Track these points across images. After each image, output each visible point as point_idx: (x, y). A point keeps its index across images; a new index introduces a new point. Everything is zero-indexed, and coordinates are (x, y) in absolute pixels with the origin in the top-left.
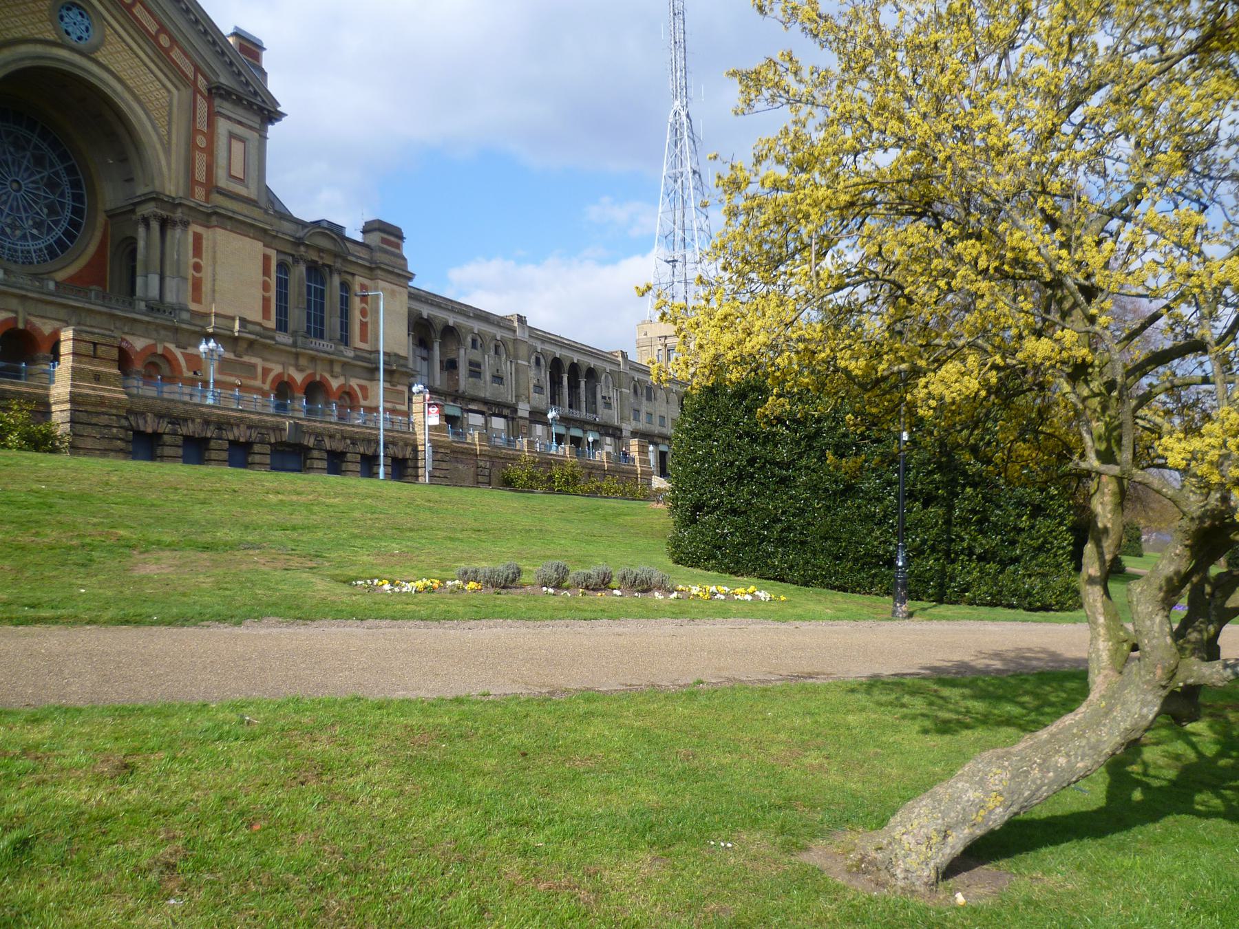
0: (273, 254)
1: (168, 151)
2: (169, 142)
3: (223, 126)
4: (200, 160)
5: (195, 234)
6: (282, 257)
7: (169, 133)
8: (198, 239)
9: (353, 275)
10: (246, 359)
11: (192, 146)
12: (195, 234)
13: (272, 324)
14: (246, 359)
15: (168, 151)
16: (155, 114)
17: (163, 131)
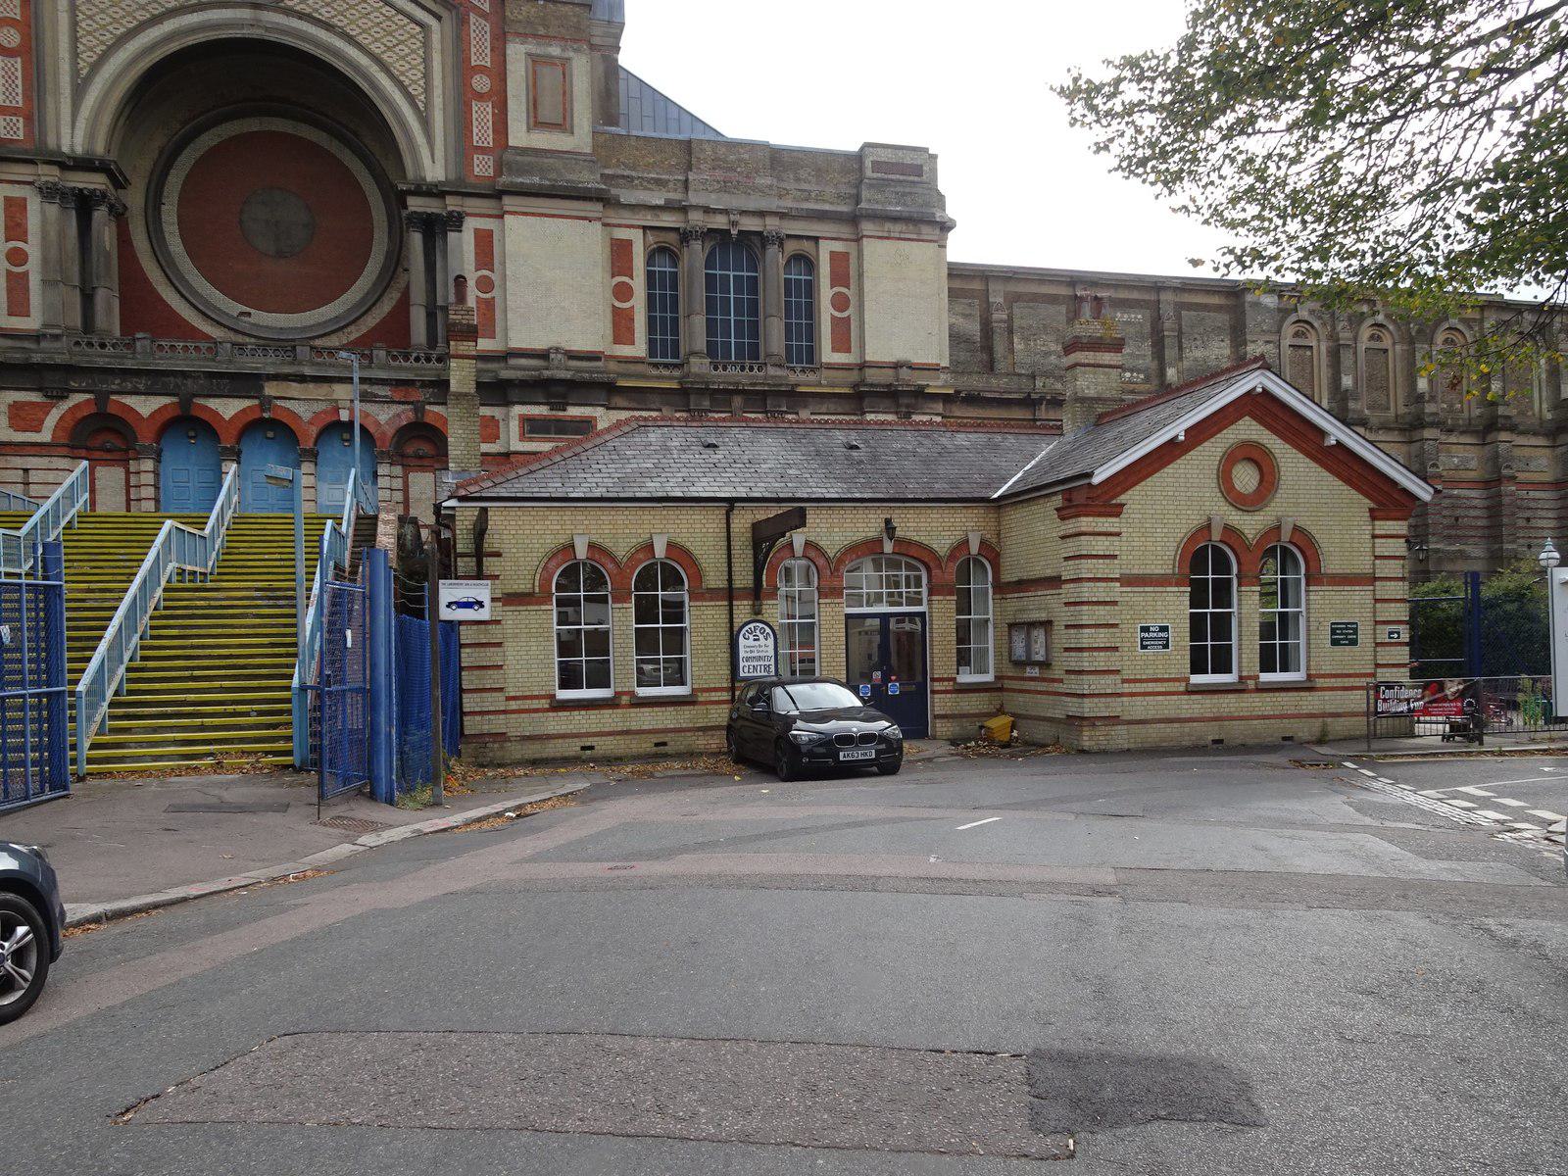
0: (637, 238)
1: (426, 122)
2: (428, 104)
3: (517, 53)
4: (482, 115)
5: (477, 231)
6: (651, 238)
7: (428, 89)
8: (484, 241)
9: (816, 239)
10: (574, 411)
11: (463, 100)
12: (477, 231)
13: (639, 348)
14: (574, 411)
15: (426, 122)
16: (397, 67)
17: (416, 90)
